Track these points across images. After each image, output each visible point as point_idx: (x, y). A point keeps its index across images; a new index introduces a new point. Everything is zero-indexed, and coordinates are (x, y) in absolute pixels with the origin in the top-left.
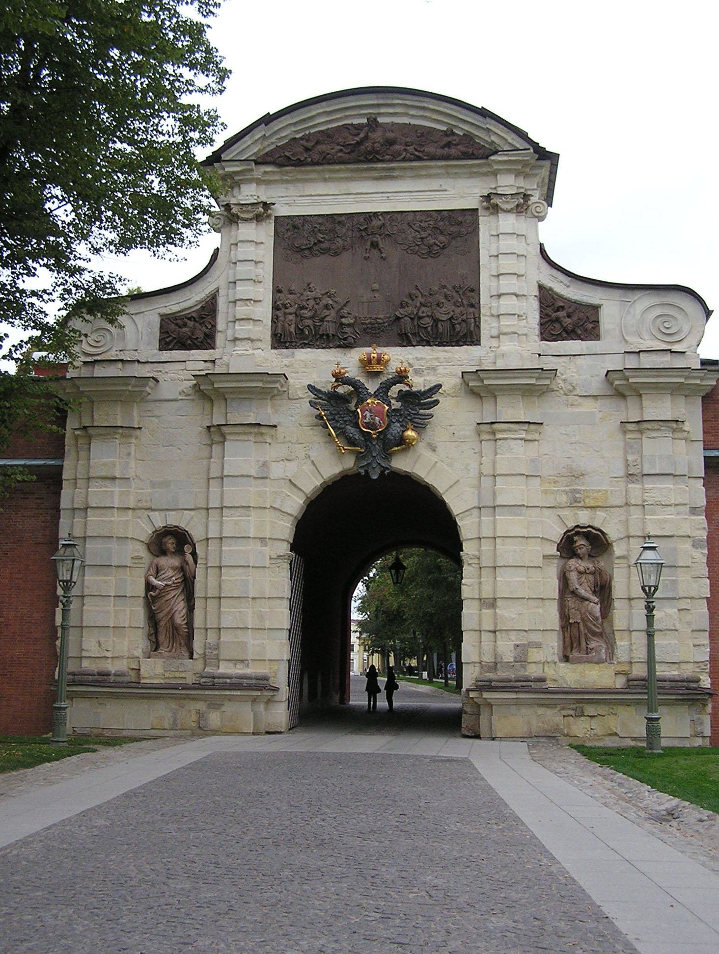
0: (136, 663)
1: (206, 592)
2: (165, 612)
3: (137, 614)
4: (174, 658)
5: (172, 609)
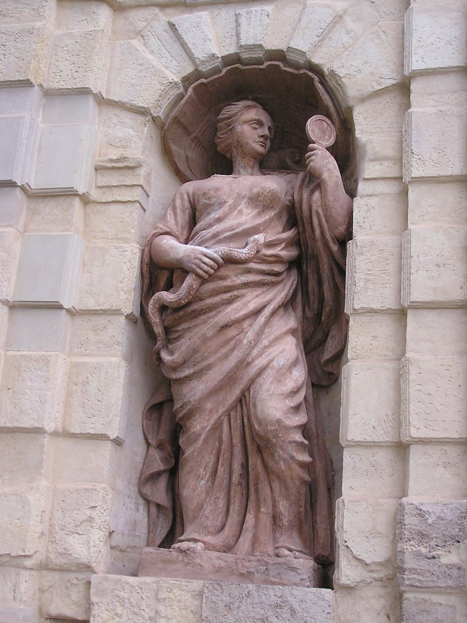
0: (76, 595)
1: (401, 285)
2: (214, 377)
3: (104, 384)
4: (247, 576)
5: (244, 364)
